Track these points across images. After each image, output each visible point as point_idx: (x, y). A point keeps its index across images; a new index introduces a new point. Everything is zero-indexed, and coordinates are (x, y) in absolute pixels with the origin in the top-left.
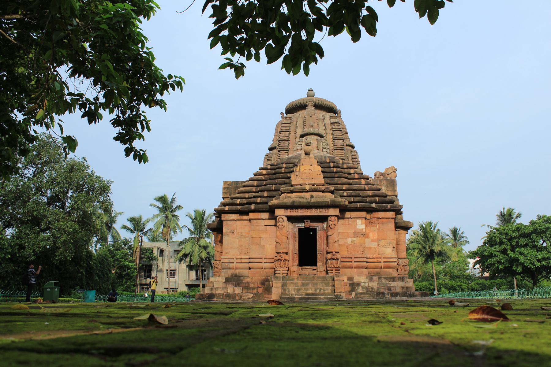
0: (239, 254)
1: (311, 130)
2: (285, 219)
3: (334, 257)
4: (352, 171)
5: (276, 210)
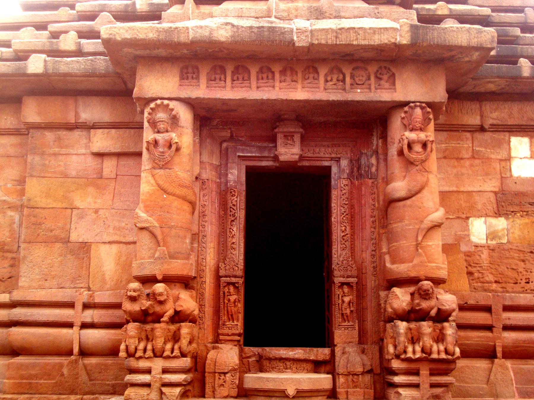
2: (185, 116)
3: (425, 305)
5: (140, 71)
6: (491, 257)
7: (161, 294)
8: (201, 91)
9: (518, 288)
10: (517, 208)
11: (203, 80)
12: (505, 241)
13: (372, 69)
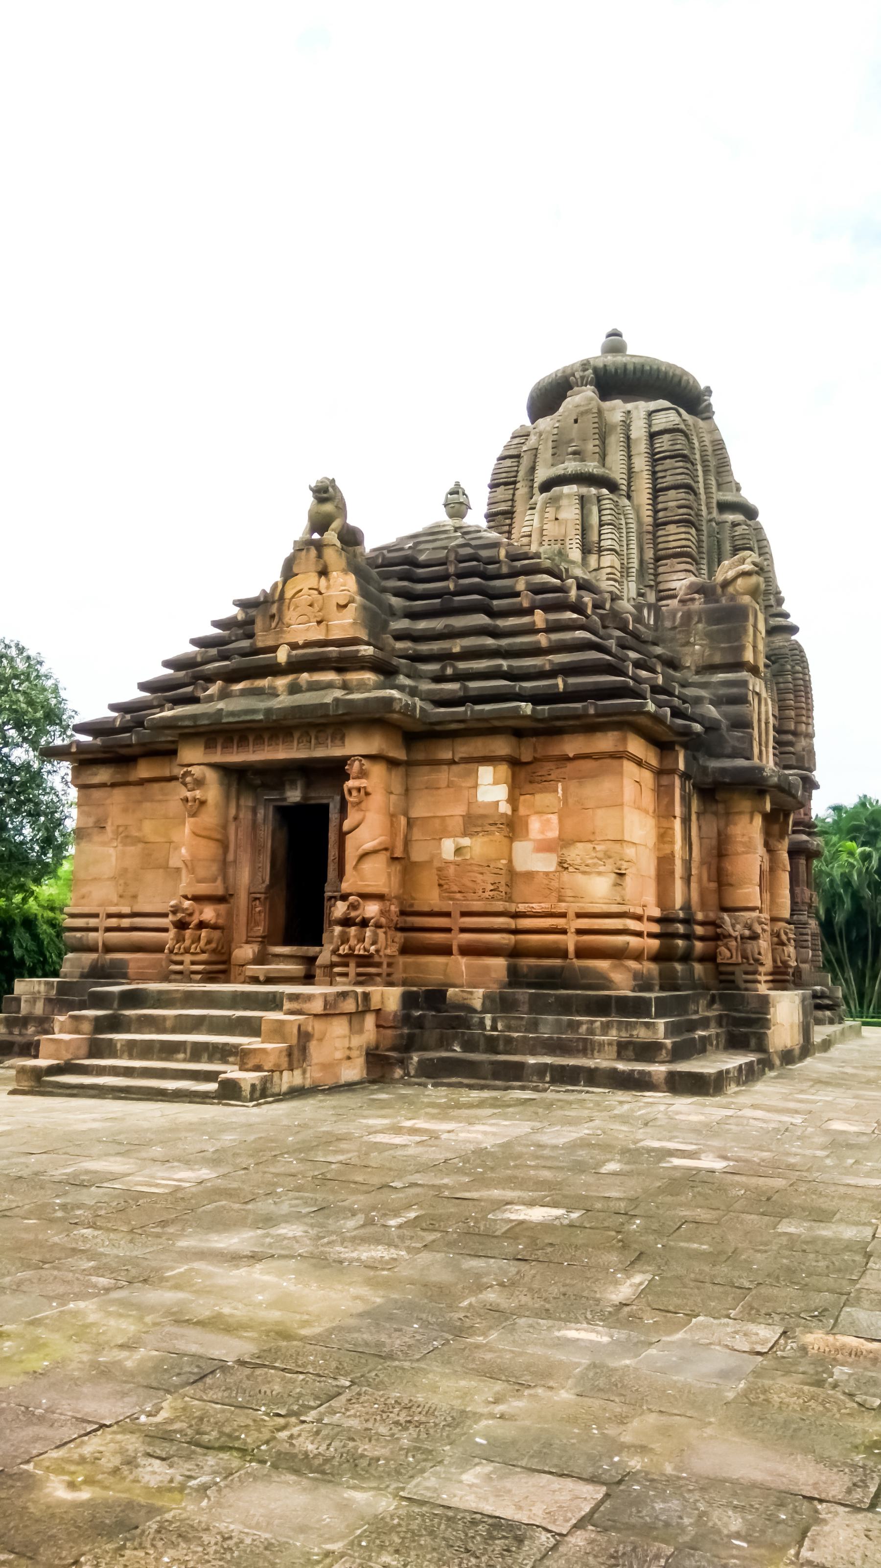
0: (115, 899)
1: (571, 466)
2: (211, 776)
3: (353, 914)
4: (521, 584)
6: (456, 870)
7: (187, 909)
8: (218, 757)
9: (475, 896)
10: (479, 829)
11: (219, 749)
12: (468, 857)
13: (330, 731)
